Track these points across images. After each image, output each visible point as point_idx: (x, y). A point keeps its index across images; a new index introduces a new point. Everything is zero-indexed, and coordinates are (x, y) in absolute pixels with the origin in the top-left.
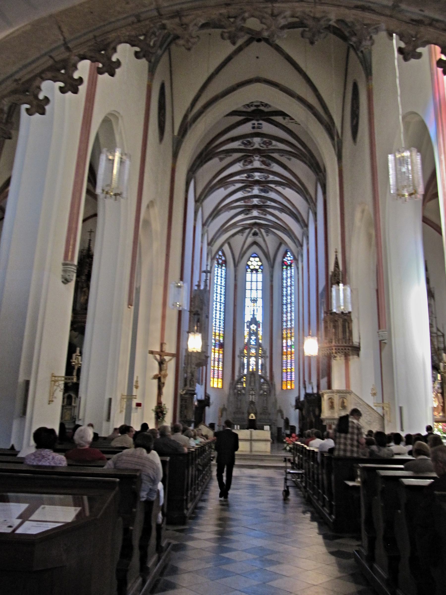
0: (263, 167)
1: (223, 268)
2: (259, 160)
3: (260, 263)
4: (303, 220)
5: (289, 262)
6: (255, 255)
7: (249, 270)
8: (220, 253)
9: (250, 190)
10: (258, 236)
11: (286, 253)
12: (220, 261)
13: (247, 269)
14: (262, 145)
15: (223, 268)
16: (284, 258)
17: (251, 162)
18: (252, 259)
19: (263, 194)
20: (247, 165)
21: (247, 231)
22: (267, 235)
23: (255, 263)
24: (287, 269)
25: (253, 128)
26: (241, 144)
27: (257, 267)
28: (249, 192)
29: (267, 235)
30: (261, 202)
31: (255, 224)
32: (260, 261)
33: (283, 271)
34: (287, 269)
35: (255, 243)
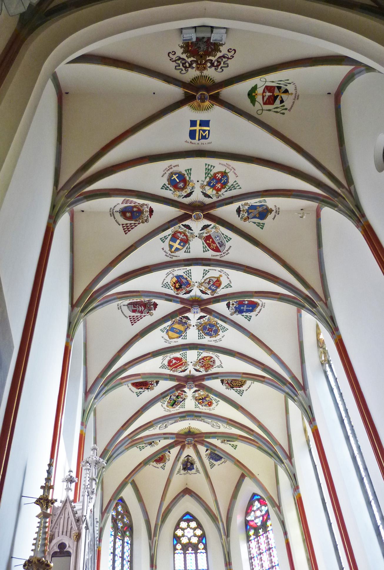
0: (210, 254)
1: (127, 539)
2: (200, 237)
3: (199, 532)
4: (294, 378)
5: (259, 522)
6: (188, 517)
7: (179, 547)
8: (120, 509)
9: (182, 328)
10: (194, 471)
11: (250, 505)
12: (120, 525)
13: (175, 547)
14: (210, 191)
15: (127, 539)
16: (247, 513)
17: (185, 242)
18: (183, 525)
19: (207, 340)
20: (177, 249)
21: (175, 451)
22: (212, 466)
23: (189, 533)
24: (257, 534)
25: (192, 135)
26: (167, 183)
27: (195, 540)
28: (180, 333)
29: (212, 466)
31: (190, 434)
32: (199, 526)
33: (248, 540)
34: (257, 534)
35: (187, 491)
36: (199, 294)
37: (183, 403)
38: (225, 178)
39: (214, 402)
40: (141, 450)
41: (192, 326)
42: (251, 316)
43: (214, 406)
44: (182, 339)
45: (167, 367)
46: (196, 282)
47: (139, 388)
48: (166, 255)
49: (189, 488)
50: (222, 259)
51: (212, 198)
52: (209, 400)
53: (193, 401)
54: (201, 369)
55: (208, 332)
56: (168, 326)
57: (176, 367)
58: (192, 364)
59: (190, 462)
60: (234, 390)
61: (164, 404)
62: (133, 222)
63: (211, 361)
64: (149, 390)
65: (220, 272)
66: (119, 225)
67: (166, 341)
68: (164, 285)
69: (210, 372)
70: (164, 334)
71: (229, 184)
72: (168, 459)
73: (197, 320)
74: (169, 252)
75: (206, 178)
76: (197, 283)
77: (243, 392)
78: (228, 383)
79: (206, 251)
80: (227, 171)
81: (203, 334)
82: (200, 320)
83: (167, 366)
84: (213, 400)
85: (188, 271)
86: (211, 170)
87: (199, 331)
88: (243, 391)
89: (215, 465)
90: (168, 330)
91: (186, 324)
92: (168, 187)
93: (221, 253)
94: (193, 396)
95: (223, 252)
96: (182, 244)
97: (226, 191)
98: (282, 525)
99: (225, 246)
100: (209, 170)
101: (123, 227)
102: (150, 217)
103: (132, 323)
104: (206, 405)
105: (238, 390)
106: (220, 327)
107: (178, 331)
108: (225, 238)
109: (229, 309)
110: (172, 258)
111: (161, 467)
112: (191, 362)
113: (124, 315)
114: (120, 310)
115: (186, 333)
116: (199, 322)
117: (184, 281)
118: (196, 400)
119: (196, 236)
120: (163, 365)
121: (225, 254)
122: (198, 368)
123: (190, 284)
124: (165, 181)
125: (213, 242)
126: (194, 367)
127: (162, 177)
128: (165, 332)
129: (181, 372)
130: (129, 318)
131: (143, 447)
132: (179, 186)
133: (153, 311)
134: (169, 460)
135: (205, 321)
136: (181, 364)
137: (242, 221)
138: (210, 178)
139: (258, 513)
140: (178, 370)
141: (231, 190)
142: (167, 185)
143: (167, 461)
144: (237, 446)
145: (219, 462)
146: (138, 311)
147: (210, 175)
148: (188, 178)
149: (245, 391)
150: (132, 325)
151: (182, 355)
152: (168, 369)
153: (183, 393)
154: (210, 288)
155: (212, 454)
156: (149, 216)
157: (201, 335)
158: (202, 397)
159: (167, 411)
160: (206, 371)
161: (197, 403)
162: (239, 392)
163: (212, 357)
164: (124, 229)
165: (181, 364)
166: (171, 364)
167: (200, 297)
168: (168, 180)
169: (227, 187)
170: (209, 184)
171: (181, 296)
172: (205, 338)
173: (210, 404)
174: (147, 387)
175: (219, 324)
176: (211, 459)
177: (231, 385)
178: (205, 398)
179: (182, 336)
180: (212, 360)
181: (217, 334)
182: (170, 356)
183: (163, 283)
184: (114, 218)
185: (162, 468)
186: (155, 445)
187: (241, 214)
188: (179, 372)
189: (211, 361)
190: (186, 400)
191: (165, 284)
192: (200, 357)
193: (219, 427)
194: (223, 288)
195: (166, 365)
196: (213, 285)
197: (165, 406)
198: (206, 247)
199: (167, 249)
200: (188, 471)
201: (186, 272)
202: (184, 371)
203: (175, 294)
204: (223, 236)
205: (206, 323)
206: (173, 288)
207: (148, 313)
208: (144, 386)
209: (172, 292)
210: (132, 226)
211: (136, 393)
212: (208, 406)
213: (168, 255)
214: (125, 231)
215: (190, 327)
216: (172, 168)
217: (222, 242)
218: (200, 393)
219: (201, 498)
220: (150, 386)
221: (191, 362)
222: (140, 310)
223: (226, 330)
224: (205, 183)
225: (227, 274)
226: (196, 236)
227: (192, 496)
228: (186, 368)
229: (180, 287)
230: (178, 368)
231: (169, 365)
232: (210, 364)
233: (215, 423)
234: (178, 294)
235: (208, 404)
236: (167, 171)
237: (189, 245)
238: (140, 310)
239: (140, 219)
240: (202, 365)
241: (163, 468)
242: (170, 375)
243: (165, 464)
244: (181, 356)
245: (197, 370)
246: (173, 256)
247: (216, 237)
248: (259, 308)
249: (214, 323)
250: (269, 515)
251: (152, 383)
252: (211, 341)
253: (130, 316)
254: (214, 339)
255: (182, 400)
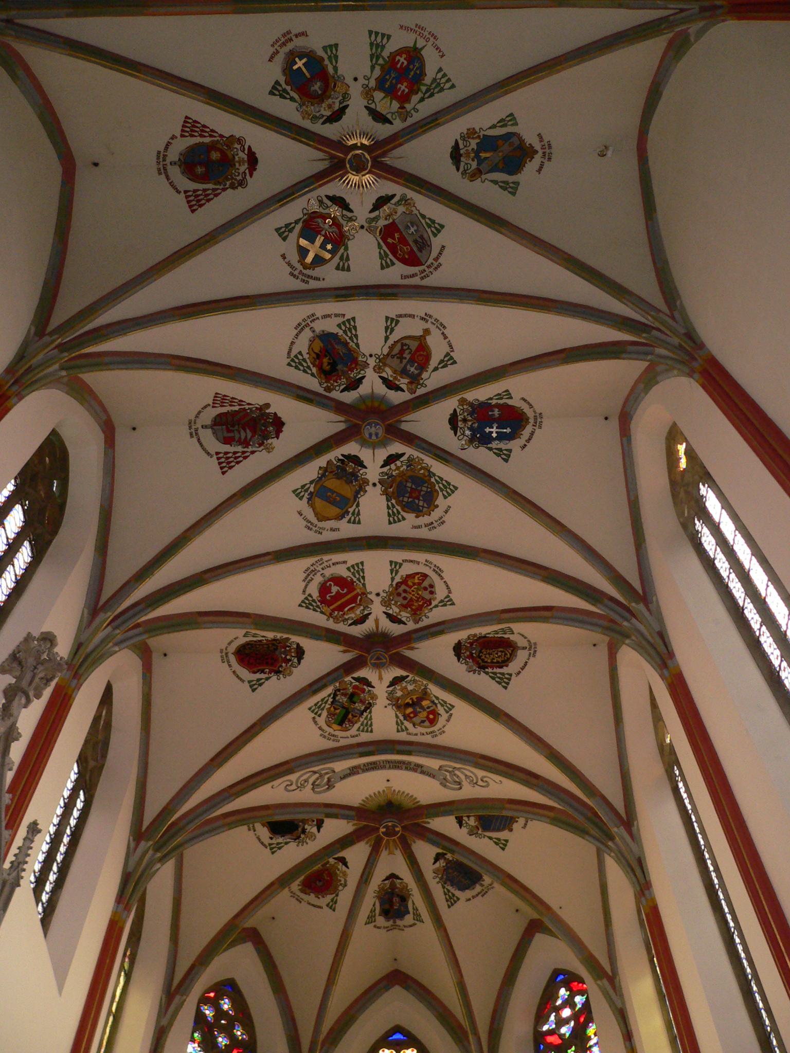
8: (226, 1005)
9: (347, 491)
10: (409, 919)
14: (384, 104)
16: (541, 1017)
20: (319, 261)
29: (452, 901)
30: (404, 607)
36: (381, 389)
37: (366, 718)
38: (417, 65)
39: (441, 710)
40: (273, 853)
41: (371, 484)
42: (510, 451)
43: (442, 721)
44: (349, 522)
45: (318, 606)
46: (371, 356)
47: (255, 669)
48: (292, 274)
49: (403, 970)
50: (426, 282)
51: (391, 123)
52: (428, 708)
53: (391, 712)
54: (404, 615)
55: (410, 500)
56: (311, 482)
57: (341, 608)
58: (380, 599)
59: (398, 895)
60: (487, 673)
61: (319, 716)
62: (210, 186)
63: (425, 589)
64: (281, 676)
65: (423, 322)
66: (179, 192)
67: (309, 525)
68: (293, 360)
69: (425, 622)
70: (303, 505)
71: (428, 80)
72: (343, 882)
73: (382, 467)
74: (300, 267)
75: (373, 68)
76: (374, 358)
77: (509, 679)
78: (471, 656)
79: (388, 266)
80: (419, 46)
81: (399, 508)
82: (388, 467)
83: (319, 604)
84: (439, 706)
85: (348, 320)
86: (383, 47)
87: (388, 500)
88: (511, 675)
89: (458, 899)
90: (311, 494)
91: (356, 480)
92: (285, 90)
93: (421, 268)
94: (391, 697)
95: (428, 263)
96: (329, 247)
97: (422, 100)
98: (620, 1019)
99: (430, 246)
100: (378, 45)
101: (187, 197)
102: (251, 176)
103: (221, 468)
104: (423, 722)
105: (498, 675)
106: (438, 483)
107: (338, 499)
108: (429, 226)
109: (456, 435)
110: (307, 282)
111: (327, 905)
112: (378, 595)
113: (204, 449)
114: (195, 440)
115: (358, 505)
116: (387, 474)
117: (341, 350)
118: (398, 707)
119: (362, 227)
120: (306, 598)
121: (431, 270)
122: (394, 610)
123: (355, 361)
124: (275, 72)
125: (403, 240)
126: (384, 609)
127: (270, 60)
128: (305, 500)
129: (356, 623)
130: (215, 457)
131: (278, 844)
132: (312, 88)
133: (273, 441)
134: (345, 885)
135: (402, 469)
136: (353, 600)
137: (466, 181)
138: (382, 66)
139: (566, 1013)
140: (346, 617)
141: (432, 95)
142: (284, 86)
143: (340, 888)
144: (507, 841)
145: (469, 893)
146: (237, 439)
147: (381, 61)
148: (330, 70)
149: (514, 675)
150: (223, 473)
151: (352, 570)
152: (322, 612)
153: (365, 687)
154: (404, 372)
155: (450, 871)
156: (247, 171)
157: (395, 510)
158: (412, 699)
159: (329, 739)
160: (416, 622)
161: (402, 718)
162: (499, 678)
163: (425, 576)
164: (188, 202)
165: (353, 600)
166: (328, 598)
167: (383, 399)
168: (284, 71)
169: (424, 88)
170: (381, 84)
171: (335, 395)
172: (404, 519)
173: (431, 716)
174: (276, 669)
175: (434, 475)
176: (449, 883)
177: (480, 661)
178: (420, 699)
179: (348, 512)
180: (426, 584)
181: (432, 507)
182: (322, 572)
183: (289, 353)
184: (168, 178)
185: (331, 908)
186: (308, 840)
187: (462, 164)
188: (350, 622)
189: (425, 589)
190: (374, 709)
191: (296, 356)
192: (398, 579)
193: (460, 783)
194: (436, 369)
195: (315, 598)
196: (412, 361)
197: (322, 721)
198: (387, 255)
199: (294, 258)
200: (395, 922)
201: (344, 323)
202: (362, 620)
203: (321, 391)
204: (423, 221)
205: (402, 474)
206: (314, 370)
207: (260, 445)
208: (267, 664)
209: (312, 383)
210: (209, 195)
211: (249, 682)
212: (427, 723)
213: (296, 273)
214: (190, 207)
215: (367, 488)
216: (291, 40)
217: (422, 237)
218: (406, 688)
219: (429, 992)
220: (284, 665)
221: (378, 595)
222: (243, 438)
223: (449, 489)
224: (372, 83)
225: (442, 324)
226: (362, 227)
227: (407, 988)
228: (366, 612)
229: (333, 365)
230: (346, 609)
231: (323, 601)
232: (423, 599)
233: (448, 774)
234: (328, 389)
235: (428, 717)
236: (281, 46)
237: (346, 249)
238: (243, 438)
239: (228, 179)
240: (405, 602)
241: (332, 906)
242: (328, 631)
243: (337, 895)
244: (349, 574)
245: (394, 619)
246: (309, 276)
247: (408, 227)
248: (529, 429)
249: (423, 474)
250: (590, 1012)
251: (288, 657)
252: (419, 527)
253: (217, 453)
254: (425, 519)
255: (363, 708)
